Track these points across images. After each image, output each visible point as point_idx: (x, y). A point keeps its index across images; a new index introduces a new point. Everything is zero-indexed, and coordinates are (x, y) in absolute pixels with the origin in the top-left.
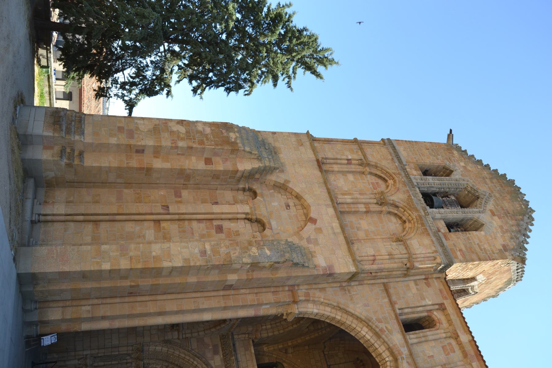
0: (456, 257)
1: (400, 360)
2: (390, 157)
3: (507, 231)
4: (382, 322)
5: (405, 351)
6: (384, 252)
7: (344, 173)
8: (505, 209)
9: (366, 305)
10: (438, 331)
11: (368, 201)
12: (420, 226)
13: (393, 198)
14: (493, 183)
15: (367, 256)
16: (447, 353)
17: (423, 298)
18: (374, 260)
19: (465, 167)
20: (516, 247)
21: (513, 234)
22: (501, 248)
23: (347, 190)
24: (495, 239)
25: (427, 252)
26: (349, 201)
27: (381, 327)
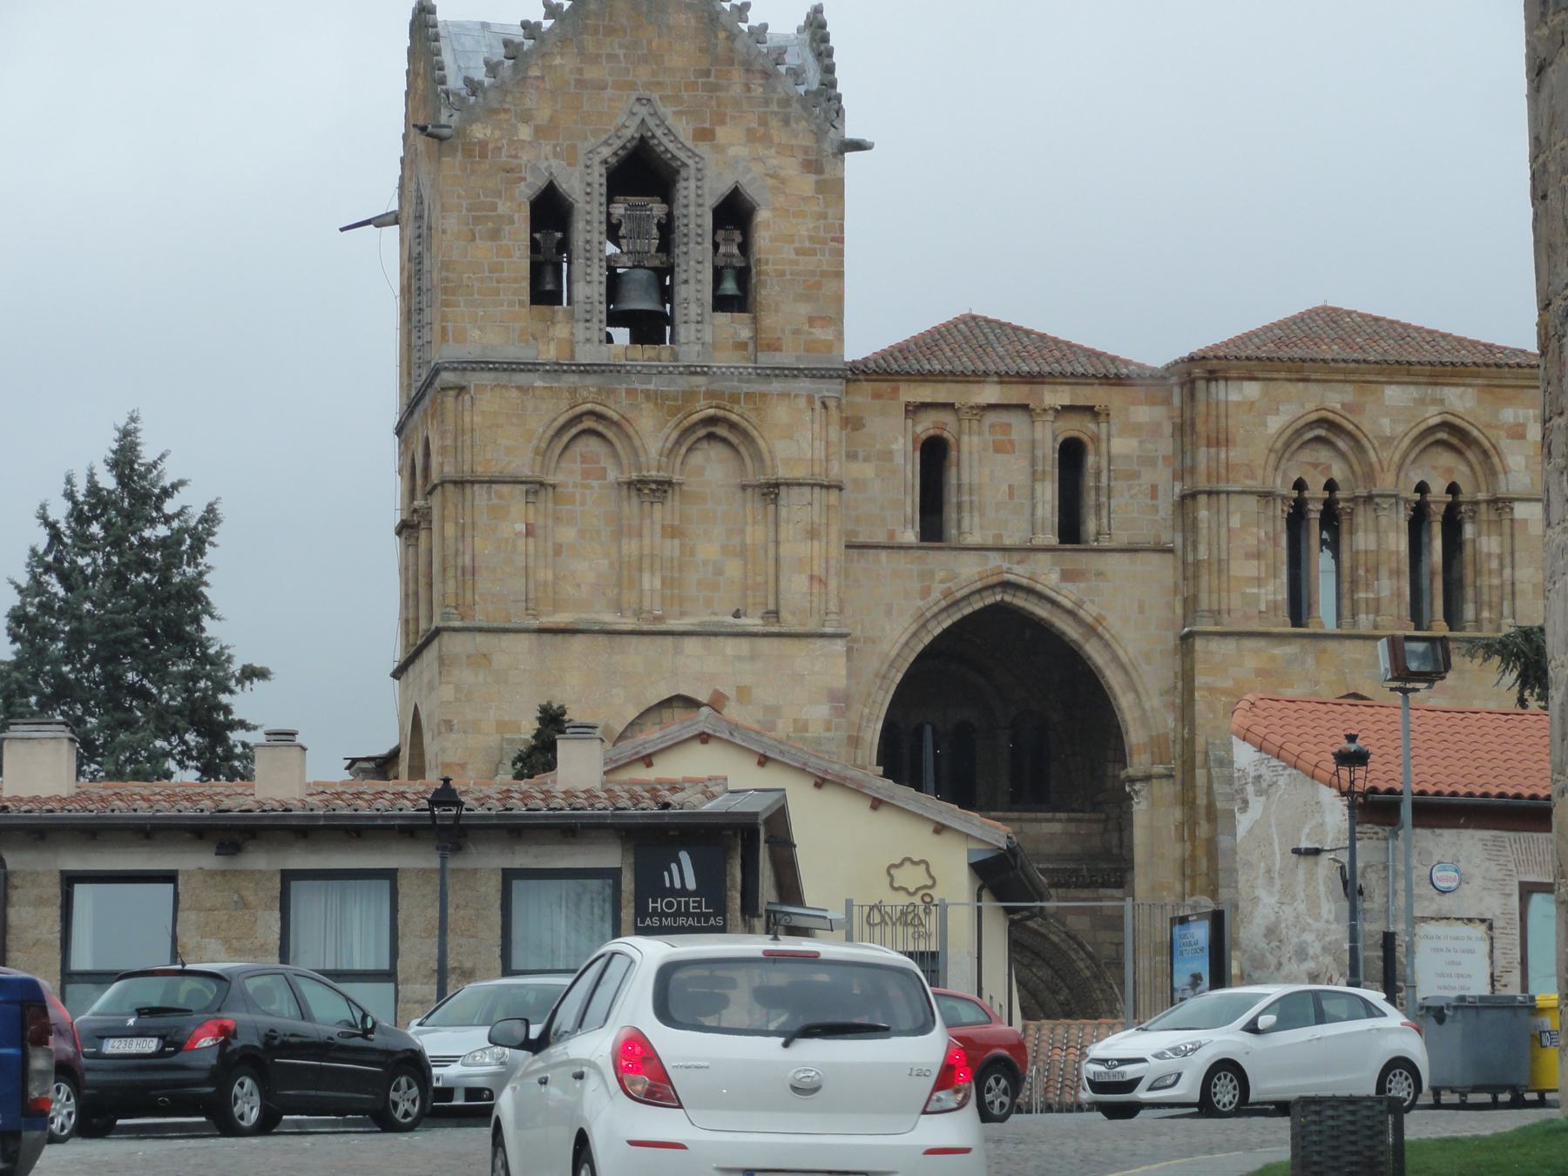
0: (829, 346)
1: (1012, 577)
2: (514, 393)
3: (763, 122)
4: (929, 588)
5: (995, 560)
6: (804, 549)
7: (558, 550)
8: (692, 79)
9: (889, 612)
10: (965, 449)
11: (658, 528)
12: (736, 408)
13: (653, 450)
14: (598, 56)
15: (811, 594)
16: (1009, 446)
17: (887, 455)
18: (821, 581)
19: (539, 132)
20: (814, 128)
21: (774, 107)
22: (812, 178)
23: (606, 562)
24: (783, 181)
25: (810, 427)
26: (657, 583)
27: (938, 595)
